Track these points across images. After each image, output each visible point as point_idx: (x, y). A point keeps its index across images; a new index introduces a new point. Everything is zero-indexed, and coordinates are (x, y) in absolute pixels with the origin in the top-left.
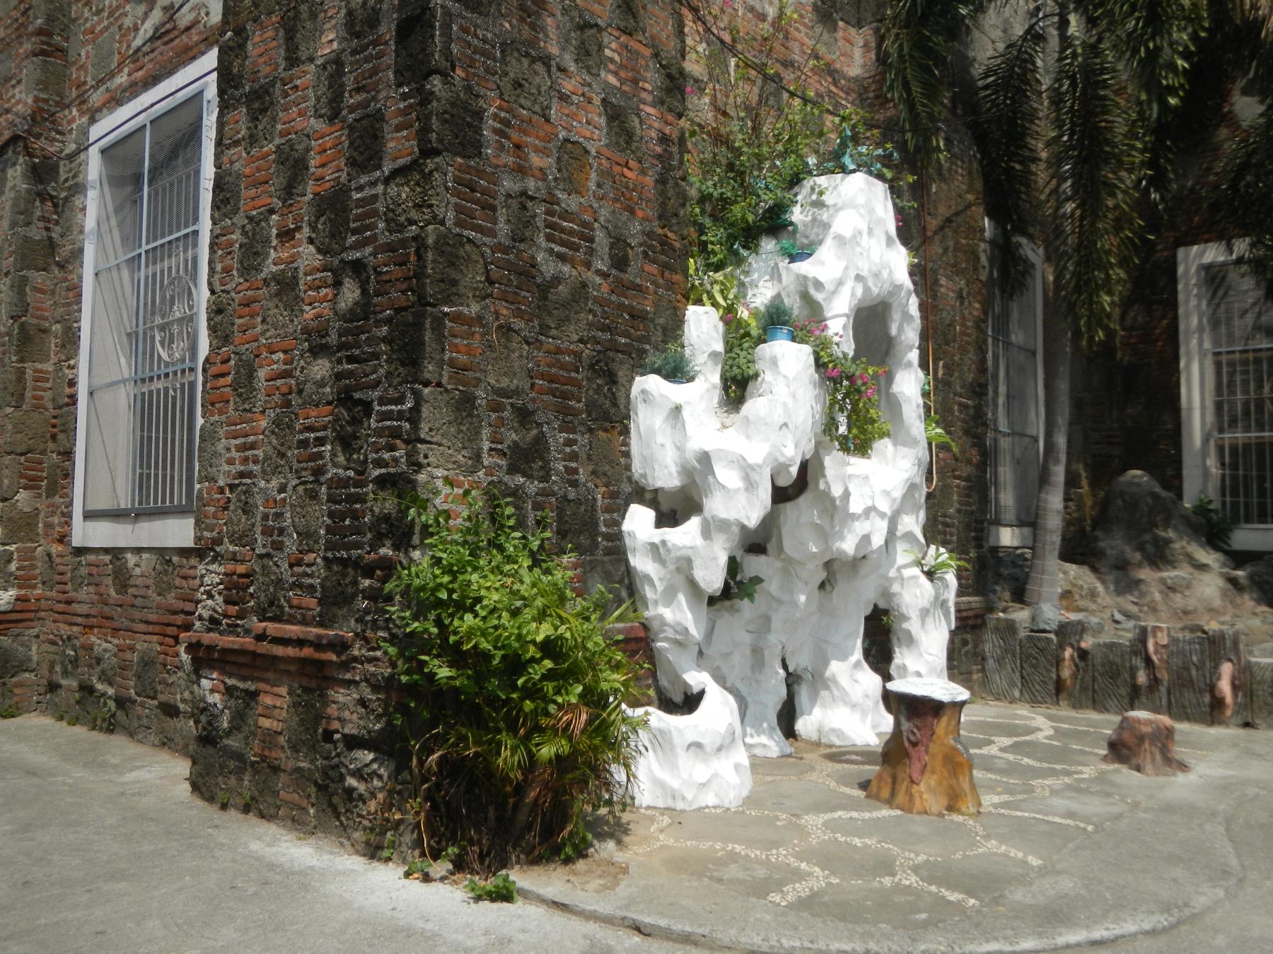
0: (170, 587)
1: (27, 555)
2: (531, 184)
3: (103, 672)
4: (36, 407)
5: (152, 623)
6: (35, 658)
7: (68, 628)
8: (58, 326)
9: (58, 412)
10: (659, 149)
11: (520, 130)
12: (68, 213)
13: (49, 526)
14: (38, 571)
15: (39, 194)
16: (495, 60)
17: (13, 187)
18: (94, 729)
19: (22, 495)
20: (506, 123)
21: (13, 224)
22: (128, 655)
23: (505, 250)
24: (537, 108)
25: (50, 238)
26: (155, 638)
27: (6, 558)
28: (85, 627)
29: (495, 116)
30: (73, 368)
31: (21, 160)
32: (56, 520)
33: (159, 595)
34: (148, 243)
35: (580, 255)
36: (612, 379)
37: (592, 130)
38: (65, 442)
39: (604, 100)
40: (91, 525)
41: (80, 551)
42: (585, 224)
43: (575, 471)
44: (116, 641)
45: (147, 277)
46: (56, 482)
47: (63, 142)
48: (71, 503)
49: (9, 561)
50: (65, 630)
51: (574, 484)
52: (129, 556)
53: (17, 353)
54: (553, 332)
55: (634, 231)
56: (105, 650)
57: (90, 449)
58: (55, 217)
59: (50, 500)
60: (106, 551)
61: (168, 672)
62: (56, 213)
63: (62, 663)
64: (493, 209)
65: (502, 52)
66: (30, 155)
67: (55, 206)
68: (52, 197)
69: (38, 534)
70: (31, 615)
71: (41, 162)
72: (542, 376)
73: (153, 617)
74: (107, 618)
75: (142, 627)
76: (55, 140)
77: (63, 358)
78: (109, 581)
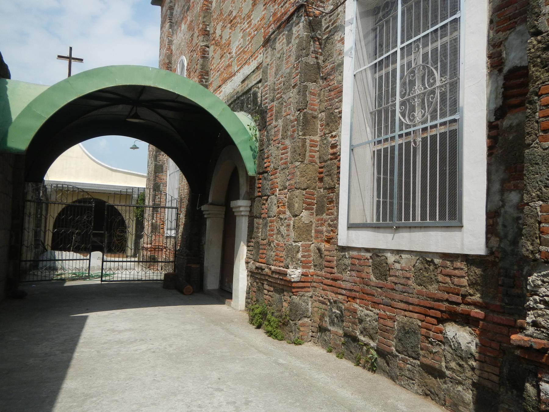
0: (431, 281)
1: (307, 249)
3: (365, 329)
4: (311, 162)
5: (412, 304)
6: (310, 310)
7: (334, 295)
8: (323, 114)
9: (323, 164)
12: (329, 46)
13: (317, 231)
14: (312, 258)
15: (312, 38)
17: (298, 37)
18: (358, 365)
19: (305, 213)
21: (298, 57)
22: (389, 323)
25: (318, 63)
26: (416, 315)
27: (297, 250)
28: (348, 297)
30: (335, 136)
31: (303, 18)
32: (324, 228)
33: (420, 285)
34: (402, 42)
38: (330, 181)
40: (354, 233)
41: (343, 249)
44: (377, 311)
45: (402, 67)
46: (323, 206)
47: (324, 7)
48: (337, 219)
49: (298, 252)
50: (332, 296)
52: (389, 255)
53: (302, 130)
56: (367, 315)
57: (352, 184)
58: (320, 51)
59: (319, 217)
60: (367, 250)
61: (431, 343)
62: (321, 48)
63: (330, 317)
66: (308, 15)
67: (320, 44)
68: (319, 39)
69: (312, 237)
70: (309, 284)
71: (313, 20)
73: (415, 300)
74: (368, 294)
75: (402, 305)
76: (319, 6)
77: (327, 132)
78: (370, 270)
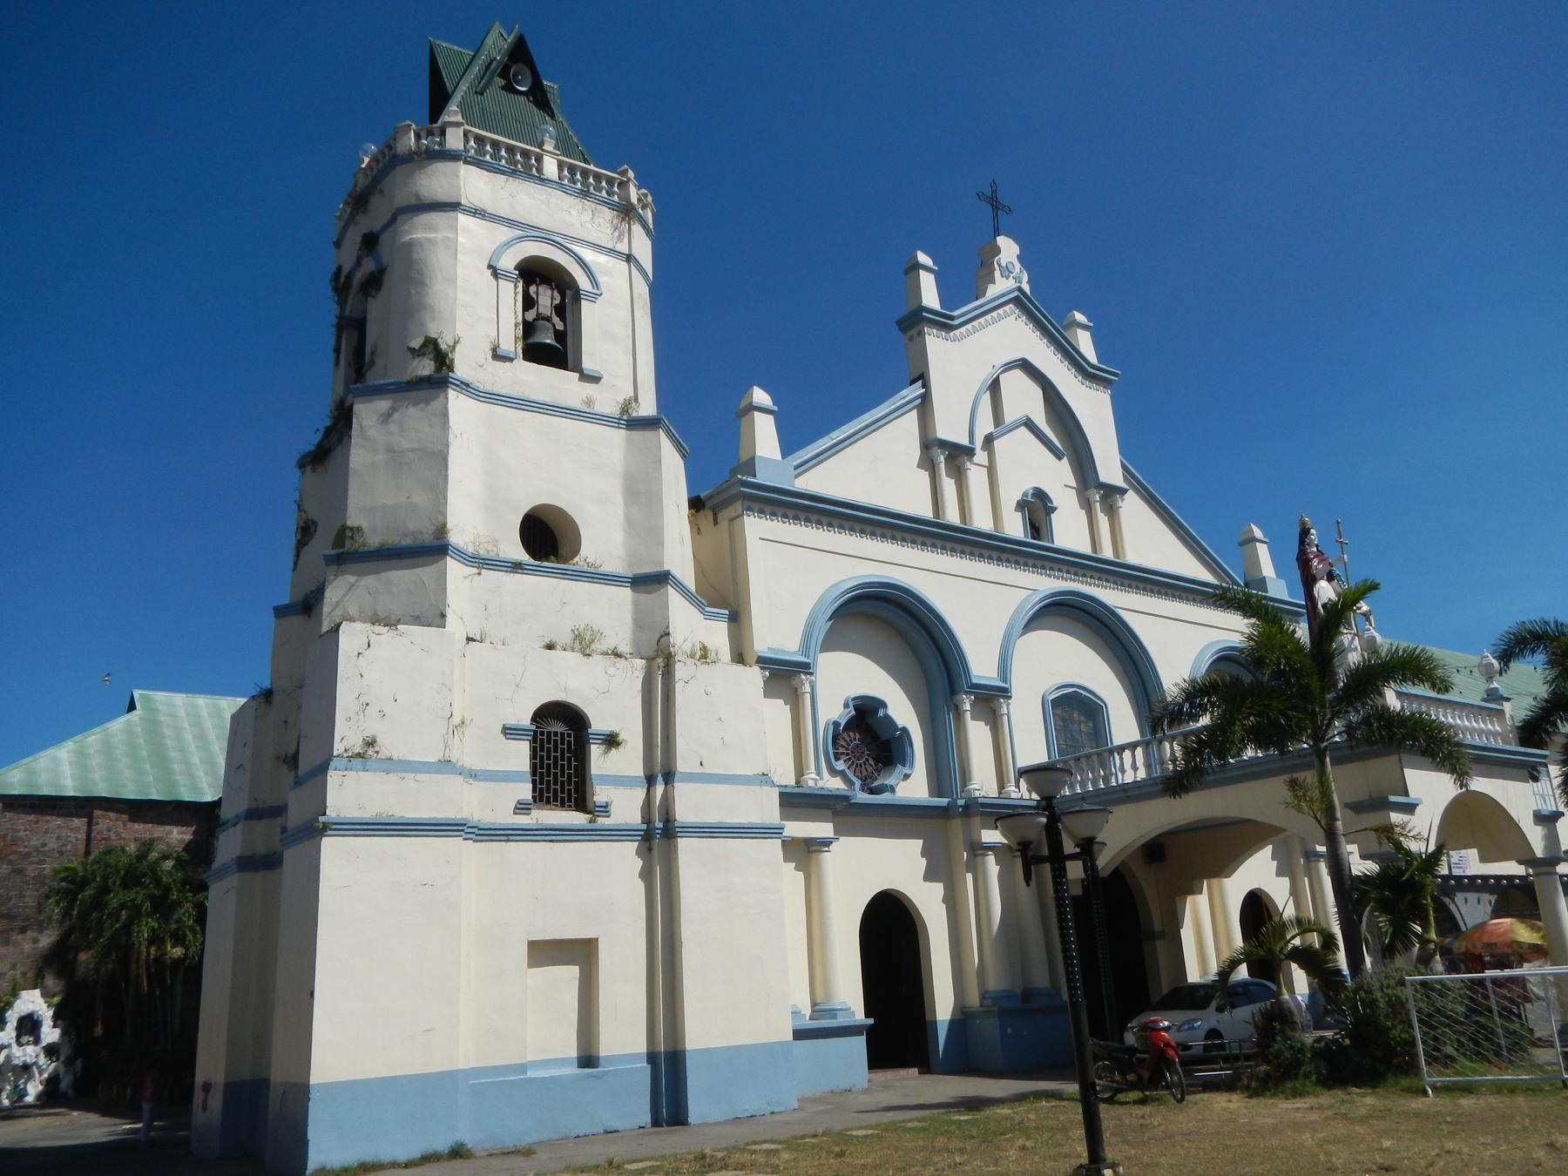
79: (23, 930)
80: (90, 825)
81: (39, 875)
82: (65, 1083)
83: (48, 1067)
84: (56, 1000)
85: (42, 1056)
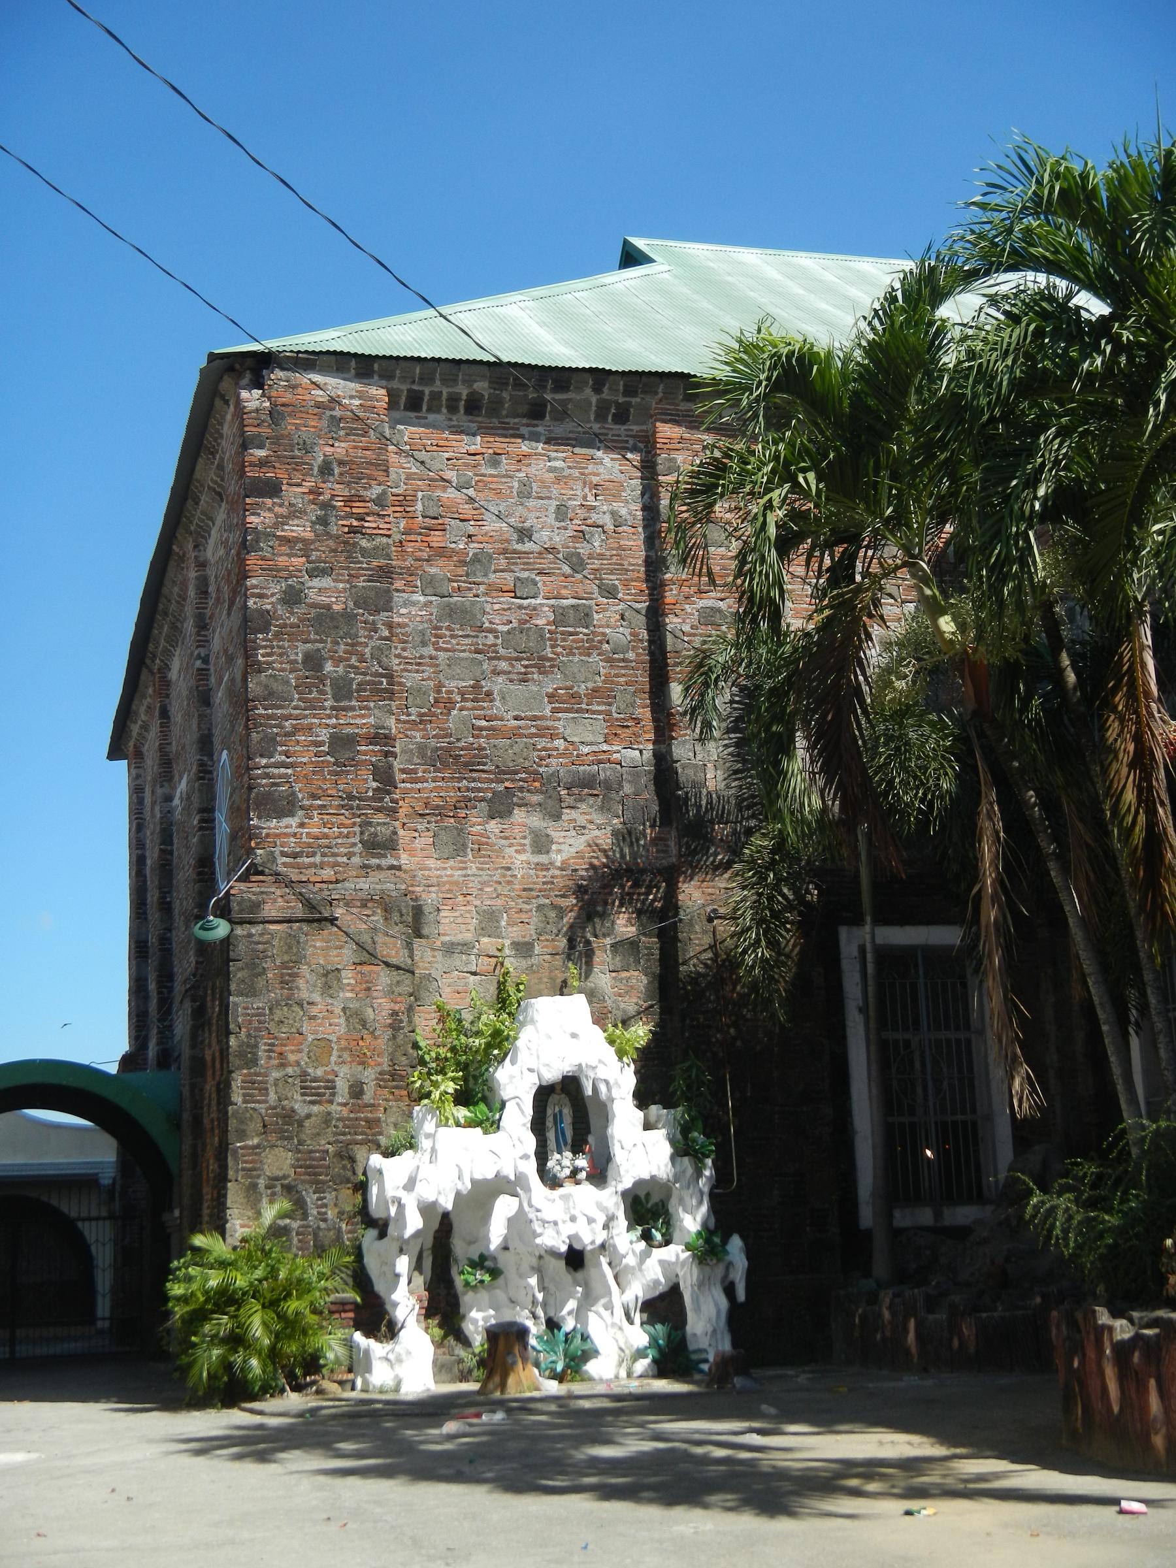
2: (290, 1070)
10: (390, 1021)
11: (282, 1045)
16: (264, 1015)
20: (272, 1045)
23: (274, 1108)
24: (294, 1030)
29: (265, 1044)
35: (327, 1097)
36: (352, 1160)
37: (337, 1028)
39: (344, 1010)
42: (328, 1081)
43: (326, 1213)
51: (325, 1220)
54: (309, 1142)
55: (369, 1076)
64: (267, 1089)
65: (270, 1009)
72: (301, 1167)
79: (500, 808)
80: (649, 469)
81: (523, 628)
82: (705, 1320)
83: (655, 1265)
84: (641, 1033)
85: (622, 1222)
